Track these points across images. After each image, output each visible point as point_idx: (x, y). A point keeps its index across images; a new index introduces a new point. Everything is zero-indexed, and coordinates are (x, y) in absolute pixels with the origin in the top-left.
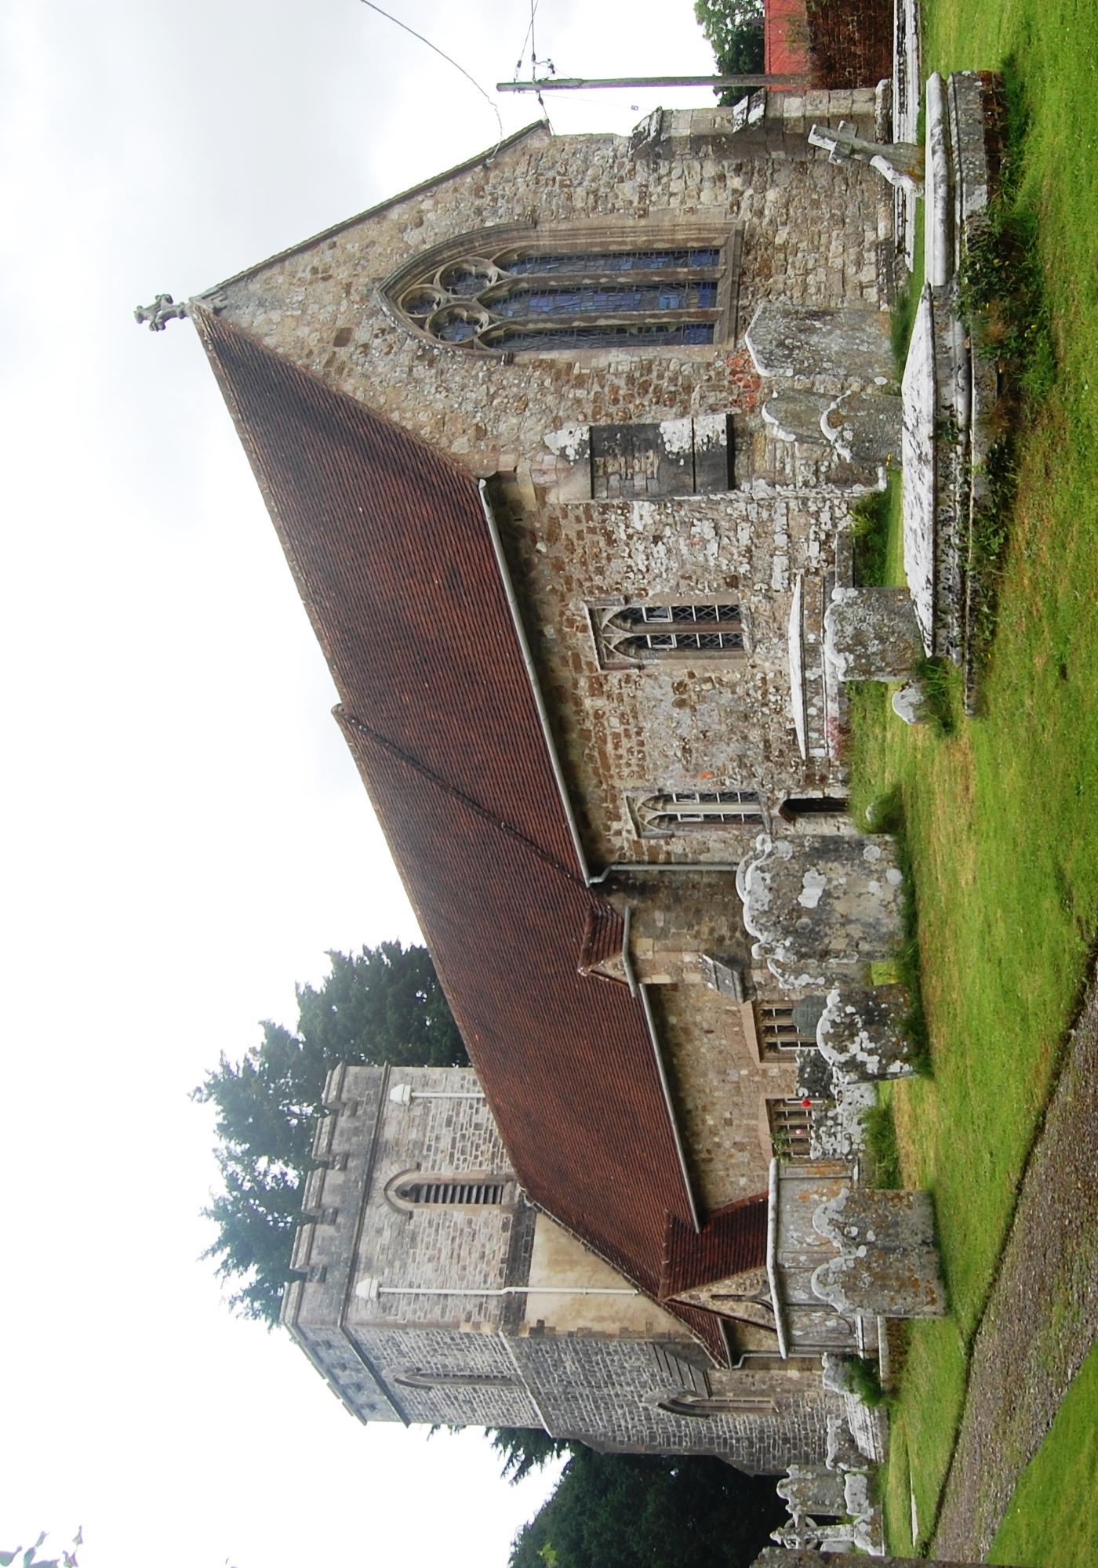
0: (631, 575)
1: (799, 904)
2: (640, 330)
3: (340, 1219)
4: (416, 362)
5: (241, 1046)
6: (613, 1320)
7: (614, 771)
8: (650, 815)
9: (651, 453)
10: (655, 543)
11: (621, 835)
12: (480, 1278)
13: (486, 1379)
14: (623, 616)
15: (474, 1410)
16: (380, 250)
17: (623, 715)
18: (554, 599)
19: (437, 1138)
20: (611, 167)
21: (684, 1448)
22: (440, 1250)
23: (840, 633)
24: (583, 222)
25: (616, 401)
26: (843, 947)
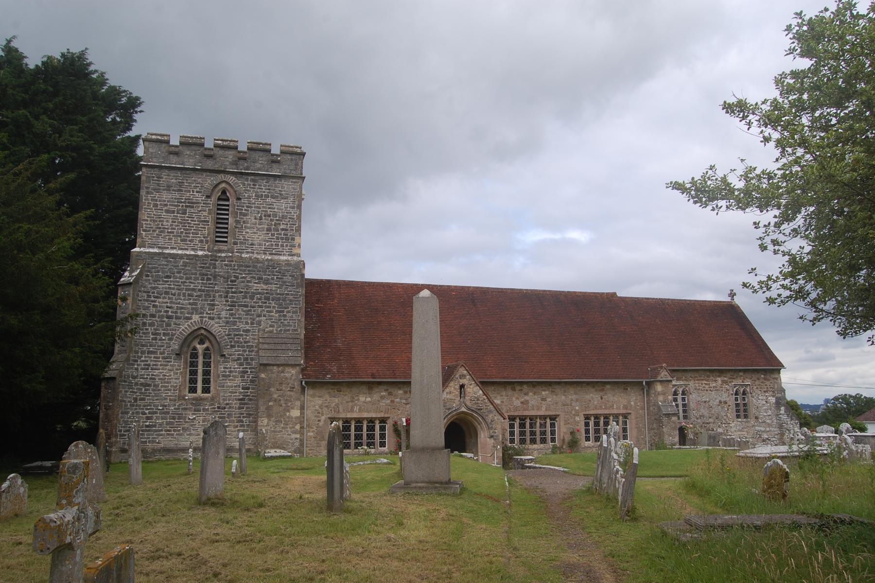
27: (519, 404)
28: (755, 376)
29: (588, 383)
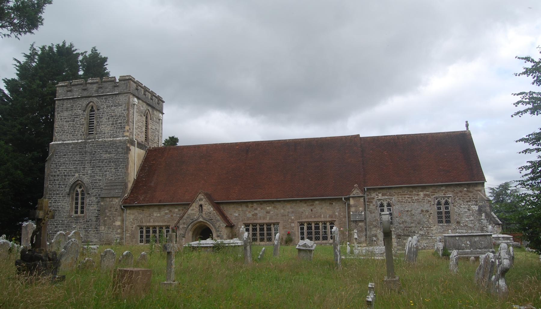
7: (400, 196)
27: (251, 216)
28: (457, 189)
29: (301, 201)
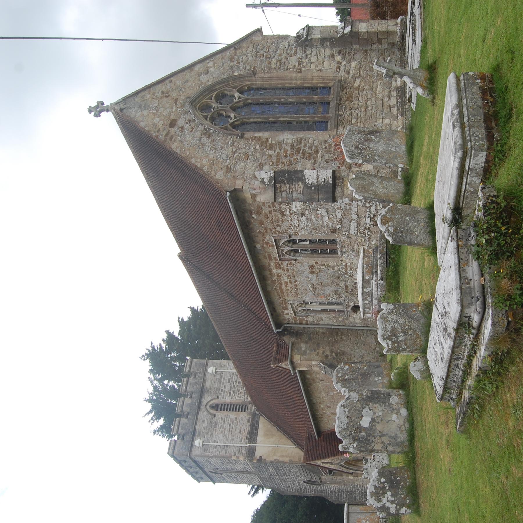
0: (292, 227)
1: (360, 425)
2: (297, 122)
3: (189, 417)
4: (203, 136)
5: (158, 340)
6: (287, 457)
8: (300, 309)
9: (300, 183)
10: (302, 216)
11: (288, 314)
12: (239, 440)
13: (242, 472)
14: (289, 241)
15: (238, 480)
16: (190, 84)
17: (289, 276)
18: (260, 235)
19: (225, 387)
20: (287, 50)
21: (312, 494)
22: (225, 429)
23: (385, 329)
24: (275, 74)
25: (286, 156)
26: (380, 448)
28: (258, 229)
